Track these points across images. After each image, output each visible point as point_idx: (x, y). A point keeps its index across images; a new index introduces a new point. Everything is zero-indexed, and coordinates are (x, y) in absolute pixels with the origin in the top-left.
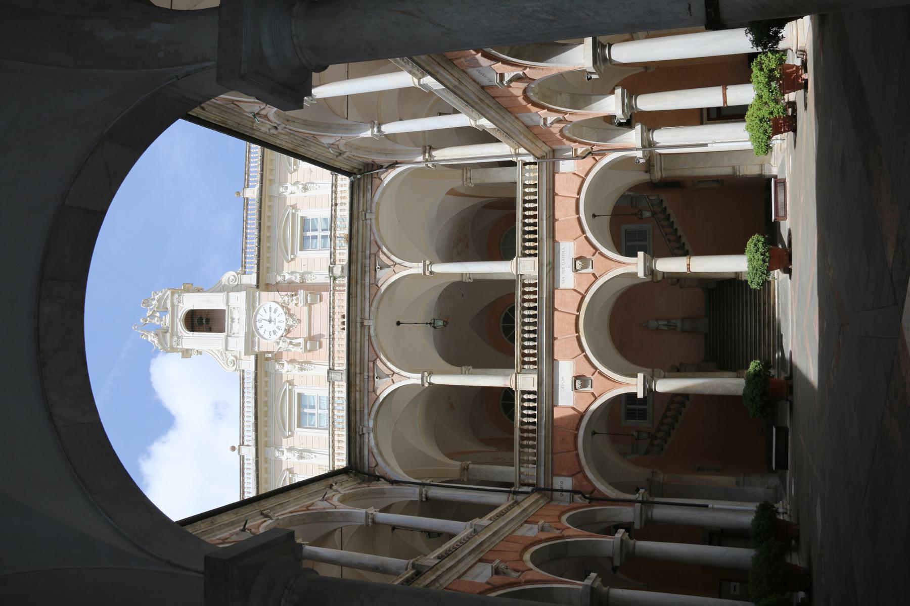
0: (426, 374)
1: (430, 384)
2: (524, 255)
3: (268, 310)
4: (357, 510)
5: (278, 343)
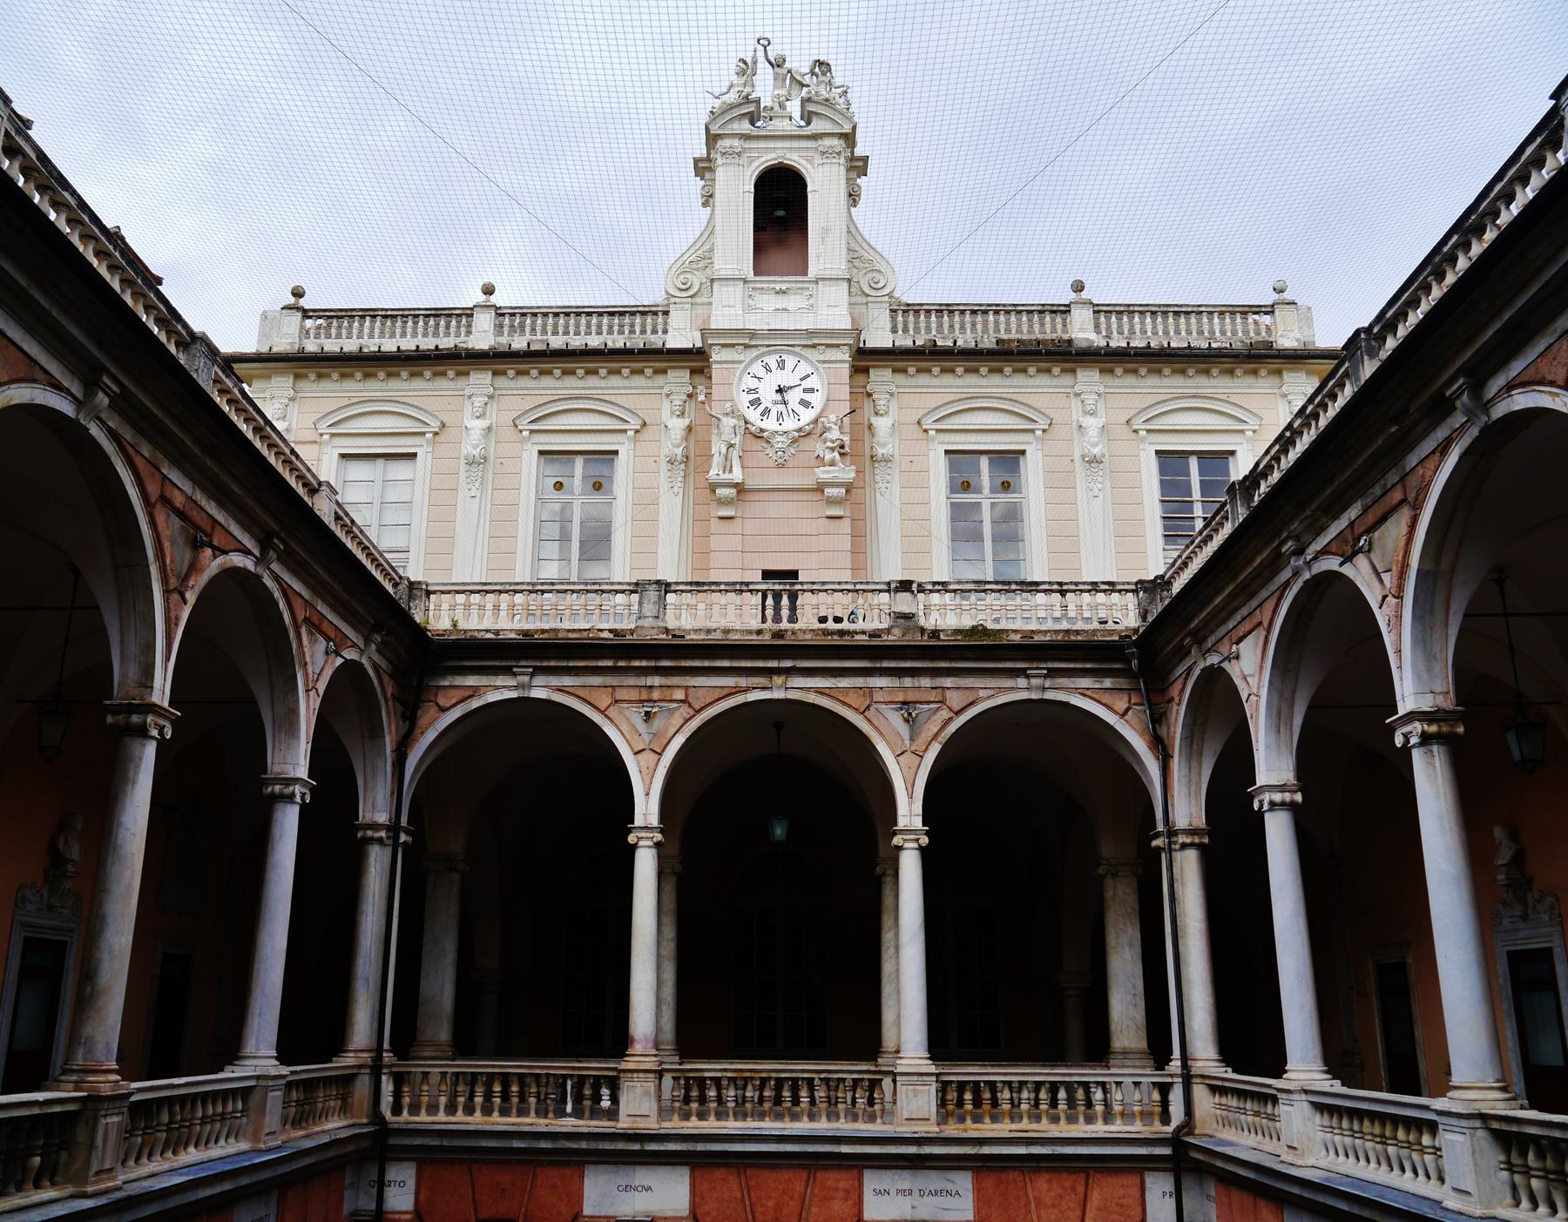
0: (659, 837)
1: (634, 847)
2: (944, 1087)
3: (807, 384)
4: (303, 747)
5: (733, 413)
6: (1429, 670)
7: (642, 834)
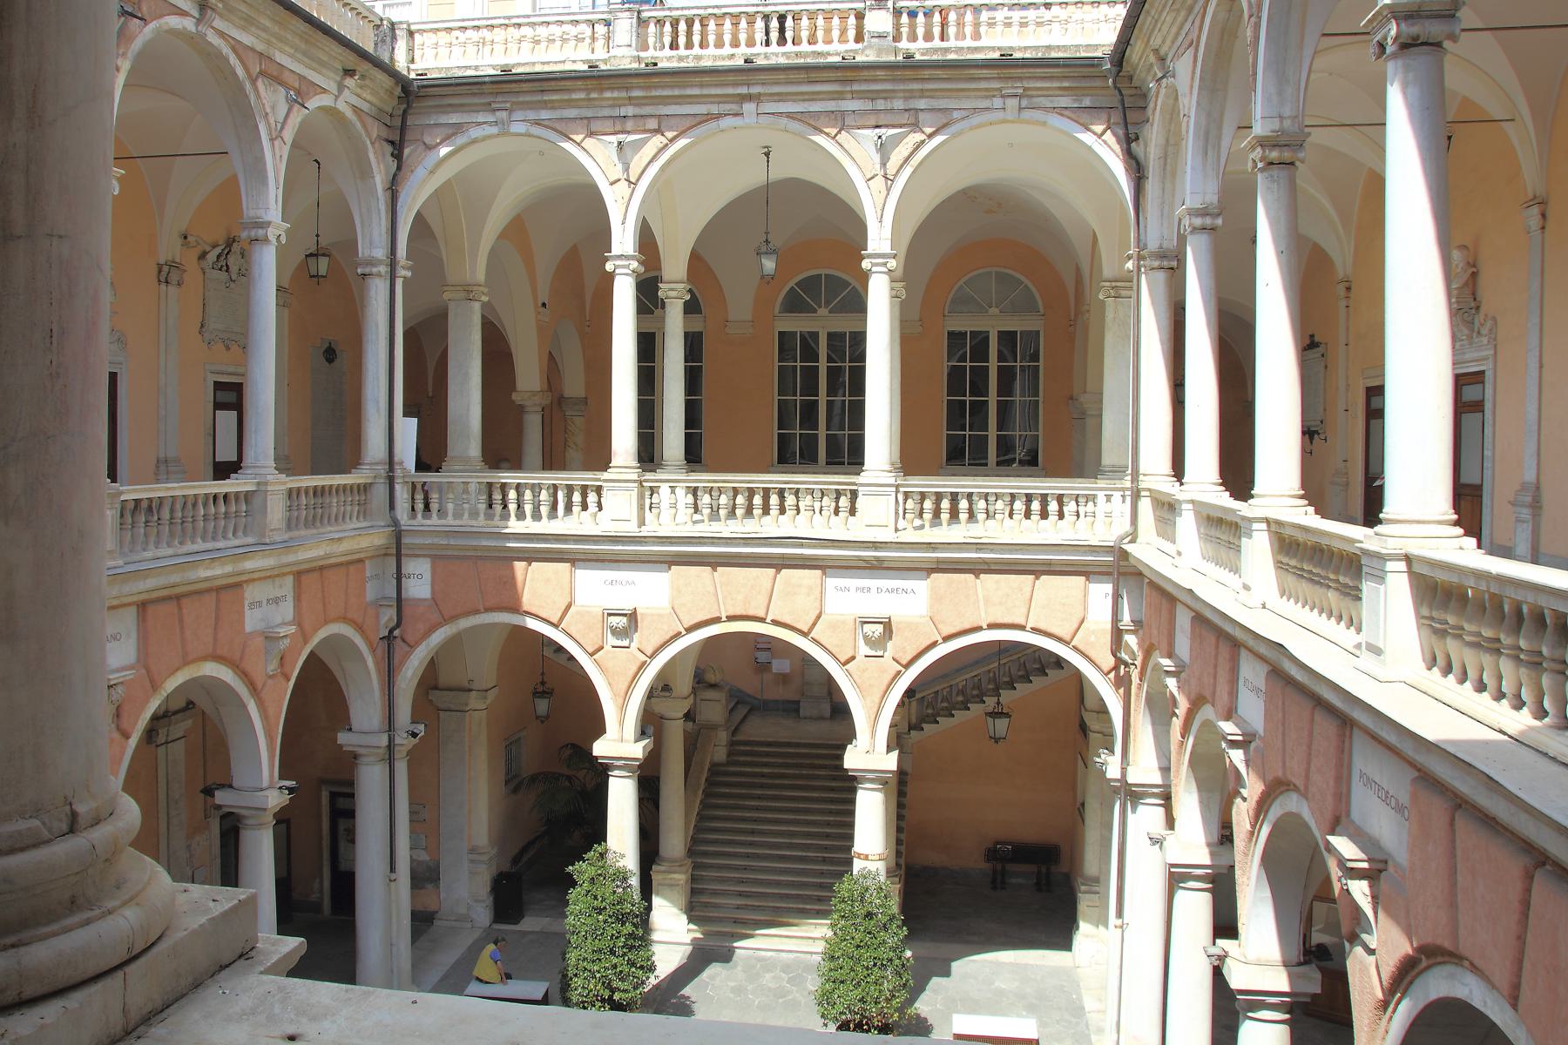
6: (1280, 93)
7: (618, 263)
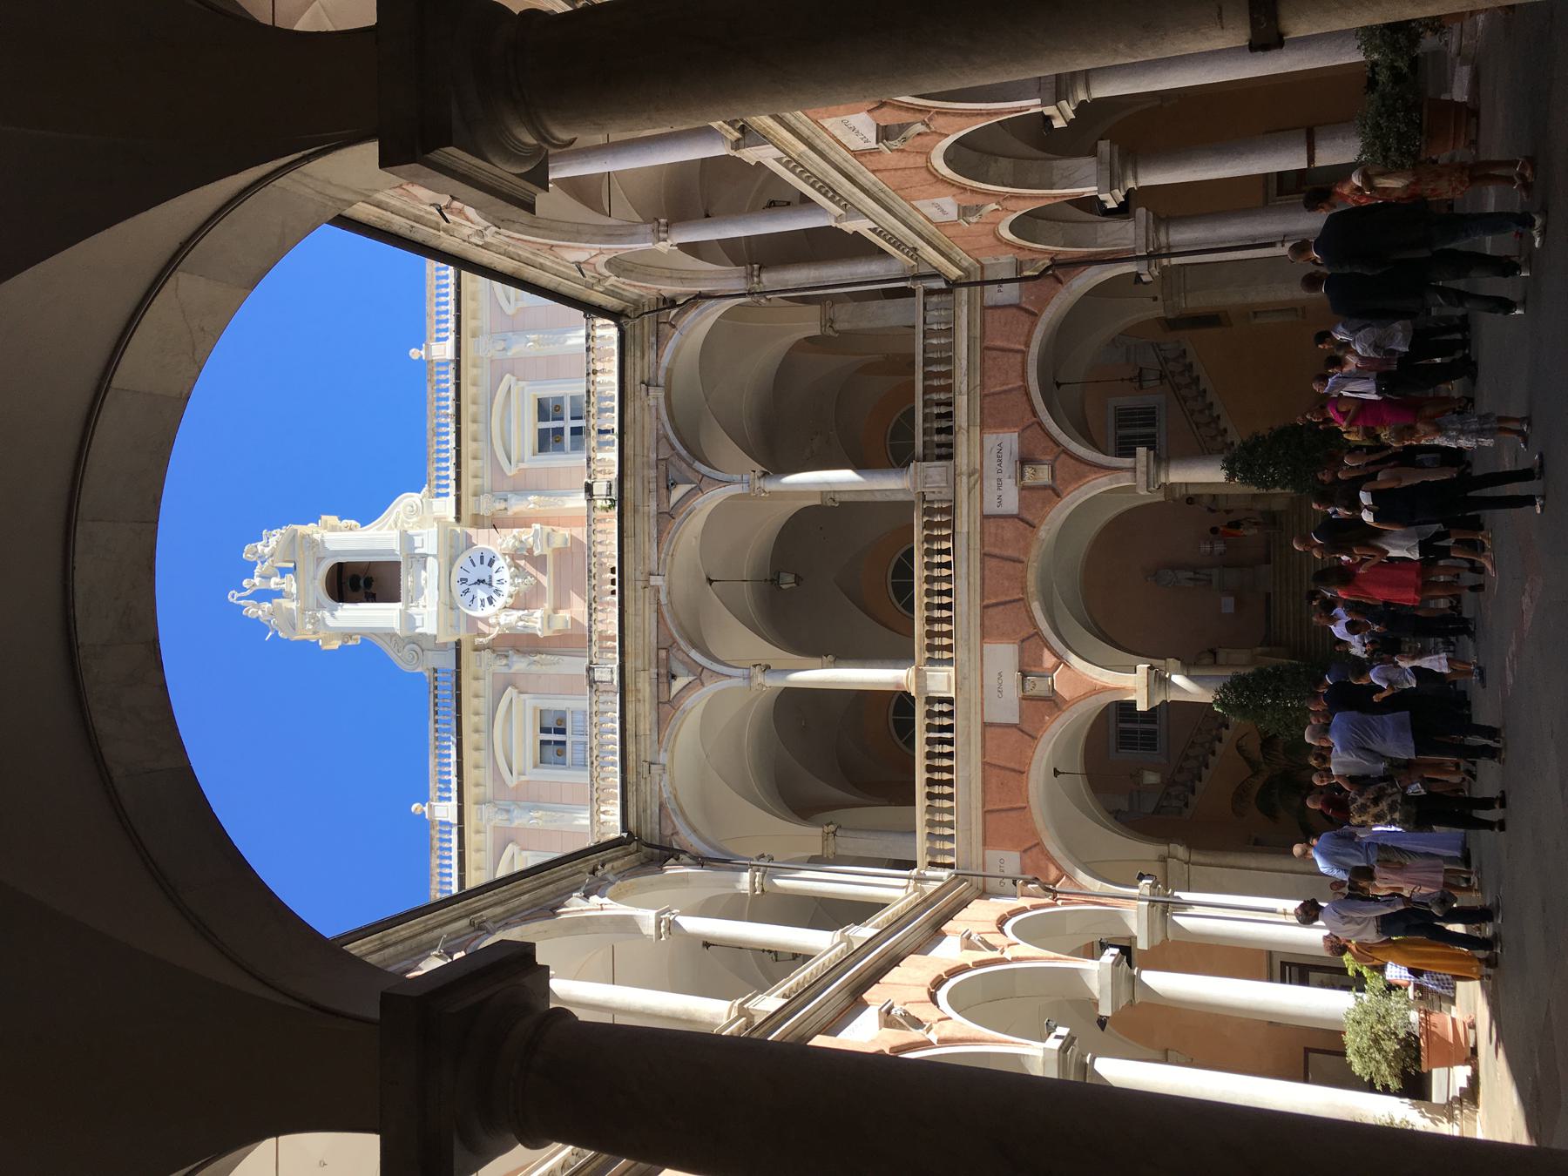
3: (477, 561)
